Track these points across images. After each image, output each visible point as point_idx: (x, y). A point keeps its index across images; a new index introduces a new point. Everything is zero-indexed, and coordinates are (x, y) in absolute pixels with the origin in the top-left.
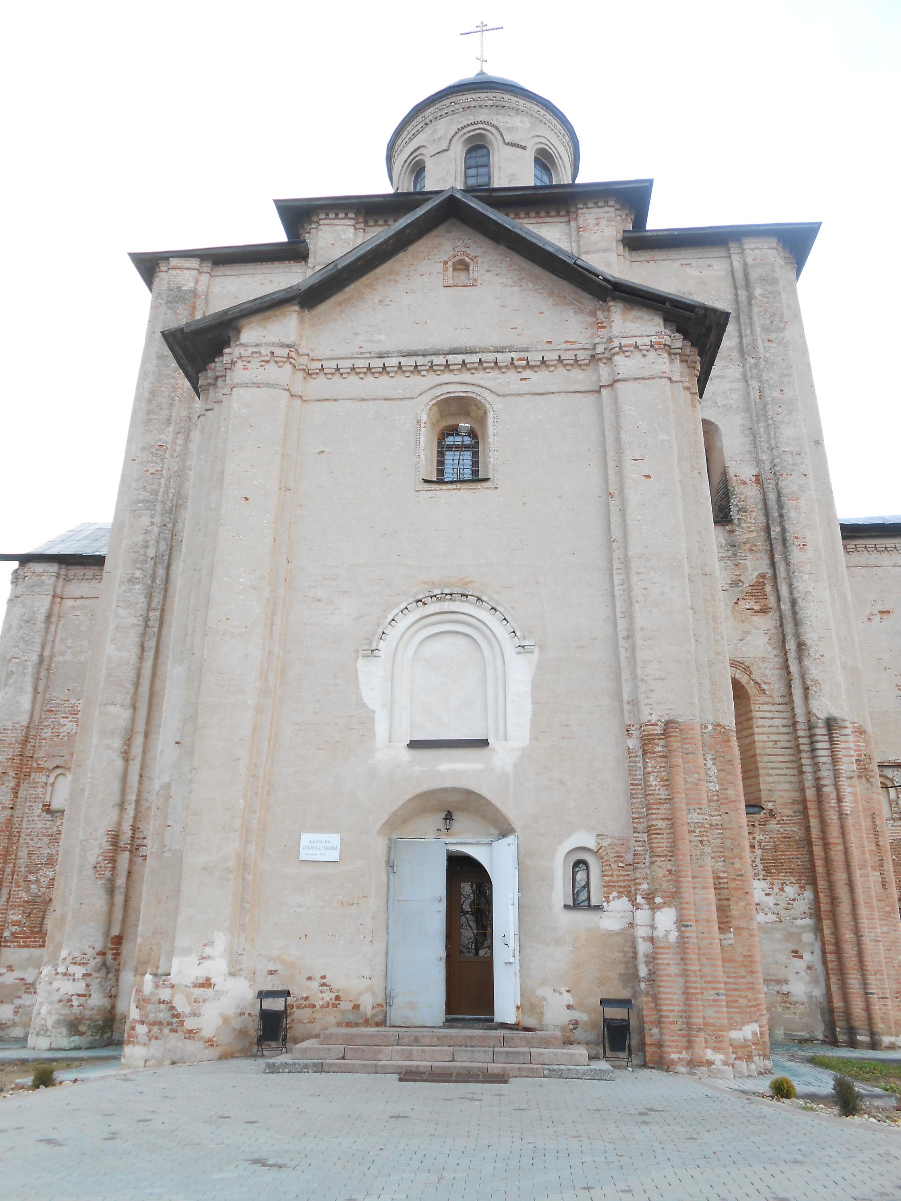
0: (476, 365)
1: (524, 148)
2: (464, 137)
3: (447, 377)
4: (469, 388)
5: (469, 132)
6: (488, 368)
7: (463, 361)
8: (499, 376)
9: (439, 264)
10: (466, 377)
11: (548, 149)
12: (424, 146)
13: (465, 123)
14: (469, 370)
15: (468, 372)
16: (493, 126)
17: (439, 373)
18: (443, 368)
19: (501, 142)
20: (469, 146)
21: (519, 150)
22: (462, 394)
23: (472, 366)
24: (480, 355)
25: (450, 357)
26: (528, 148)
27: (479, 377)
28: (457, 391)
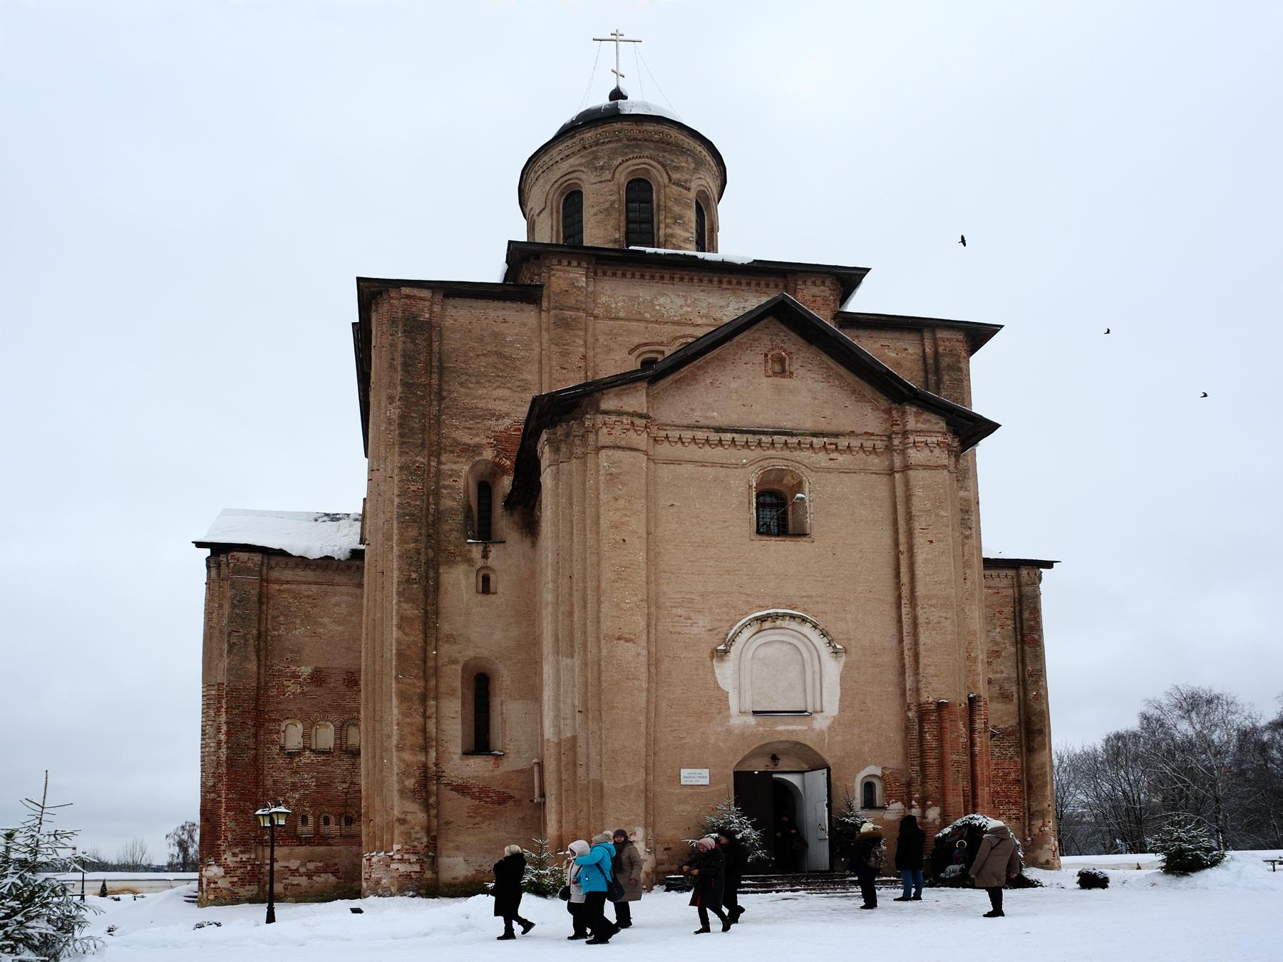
0: (796, 445)
1: (689, 189)
2: (628, 170)
3: (771, 452)
4: (790, 463)
5: (634, 165)
6: (805, 448)
7: (786, 441)
8: (813, 455)
9: (760, 356)
10: (787, 453)
11: (706, 190)
12: (582, 171)
13: (631, 156)
14: (790, 448)
15: (788, 450)
16: (659, 163)
17: (765, 448)
18: (768, 445)
19: (666, 181)
20: (631, 179)
21: (684, 191)
22: (784, 467)
23: (792, 445)
24: (800, 438)
25: (775, 437)
26: (692, 190)
27: (797, 455)
28: (780, 464)
